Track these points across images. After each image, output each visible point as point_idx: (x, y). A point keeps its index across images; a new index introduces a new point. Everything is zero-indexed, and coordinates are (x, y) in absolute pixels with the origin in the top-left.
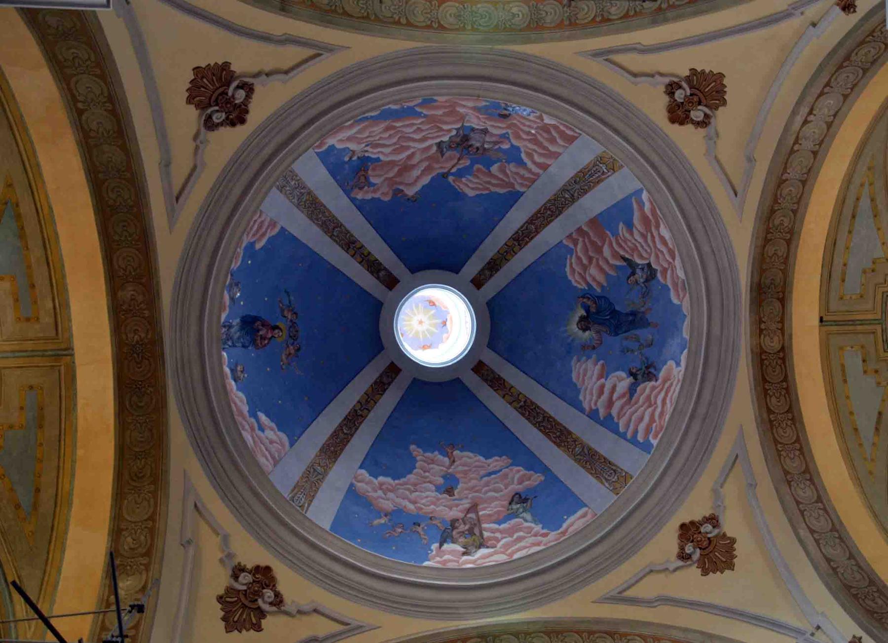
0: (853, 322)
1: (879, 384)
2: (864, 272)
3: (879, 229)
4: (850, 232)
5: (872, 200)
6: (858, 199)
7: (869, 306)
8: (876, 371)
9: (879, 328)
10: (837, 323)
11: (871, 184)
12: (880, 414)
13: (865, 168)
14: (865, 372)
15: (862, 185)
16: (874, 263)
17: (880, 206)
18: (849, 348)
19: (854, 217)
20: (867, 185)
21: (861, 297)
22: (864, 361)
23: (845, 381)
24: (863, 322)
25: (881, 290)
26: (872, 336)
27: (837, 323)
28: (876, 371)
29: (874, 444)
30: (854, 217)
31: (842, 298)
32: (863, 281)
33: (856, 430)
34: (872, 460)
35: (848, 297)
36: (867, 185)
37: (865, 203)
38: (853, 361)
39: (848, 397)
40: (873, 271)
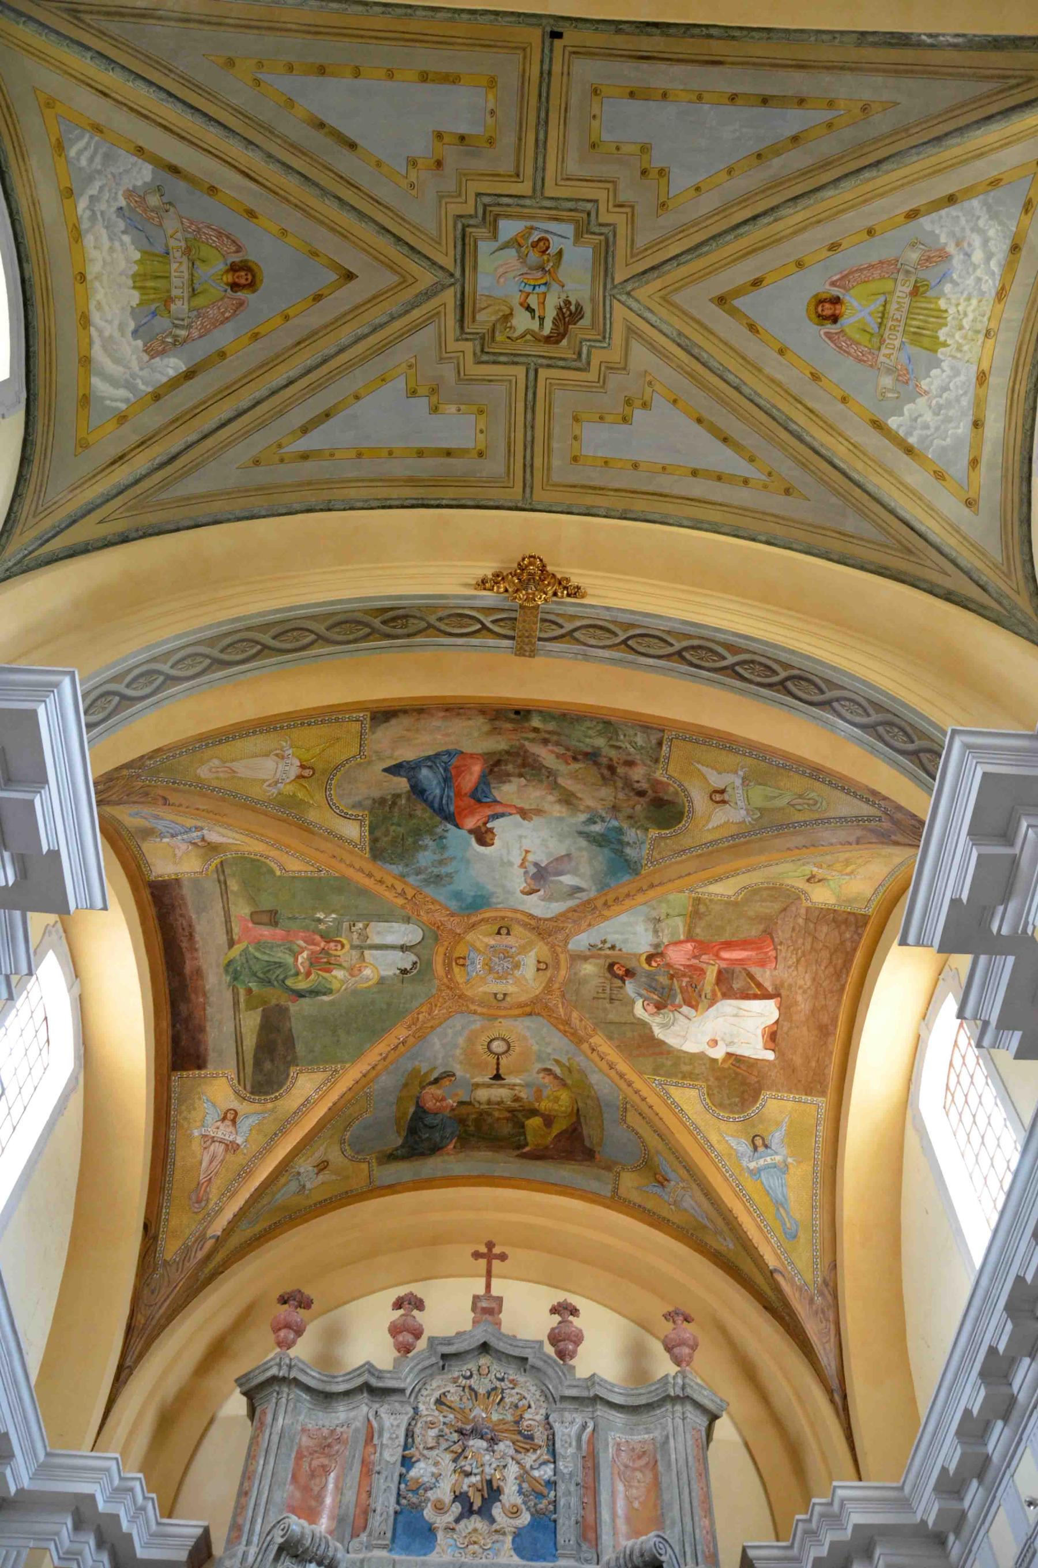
0: (543, 123)
1: (413, 163)
2: (645, 149)
3: (730, 171)
4: (733, 98)
5: (795, 139)
6: (801, 101)
7: (573, 167)
8: (439, 164)
9: (524, 188)
10: (545, 75)
11: (830, 125)
12: (353, 146)
13: (867, 95)
14: (439, 136)
15: (831, 104)
16: (662, 172)
17: (776, 162)
18: (491, 105)
19: (765, 101)
20: (827, 115)
21: (593, 146)
22: (462, 138)
23: (424, 77)
24: (541, 145)
25: (601, 195)
26: (511, 170)
27: (545, 75)
28: (439, 164)
29: (290, 103)
30: (765, 101)
31: (596, 92)
32: (625, 149)
33: (322, 71)
34: (257, 82)
35: (596, 111)
36: (827, 115)
37: (792, 121)
38: (463, 109)
39: (390, 75)
40: (644, 172)
